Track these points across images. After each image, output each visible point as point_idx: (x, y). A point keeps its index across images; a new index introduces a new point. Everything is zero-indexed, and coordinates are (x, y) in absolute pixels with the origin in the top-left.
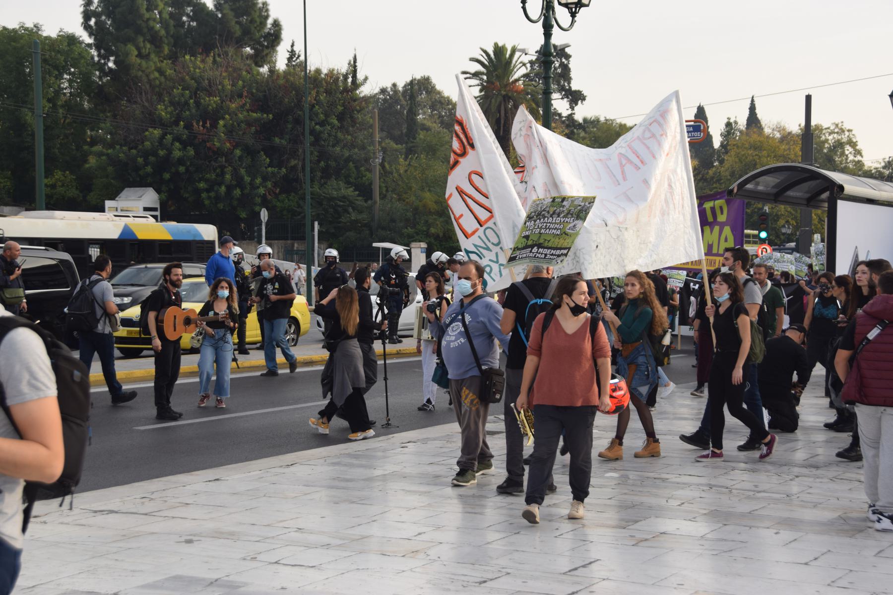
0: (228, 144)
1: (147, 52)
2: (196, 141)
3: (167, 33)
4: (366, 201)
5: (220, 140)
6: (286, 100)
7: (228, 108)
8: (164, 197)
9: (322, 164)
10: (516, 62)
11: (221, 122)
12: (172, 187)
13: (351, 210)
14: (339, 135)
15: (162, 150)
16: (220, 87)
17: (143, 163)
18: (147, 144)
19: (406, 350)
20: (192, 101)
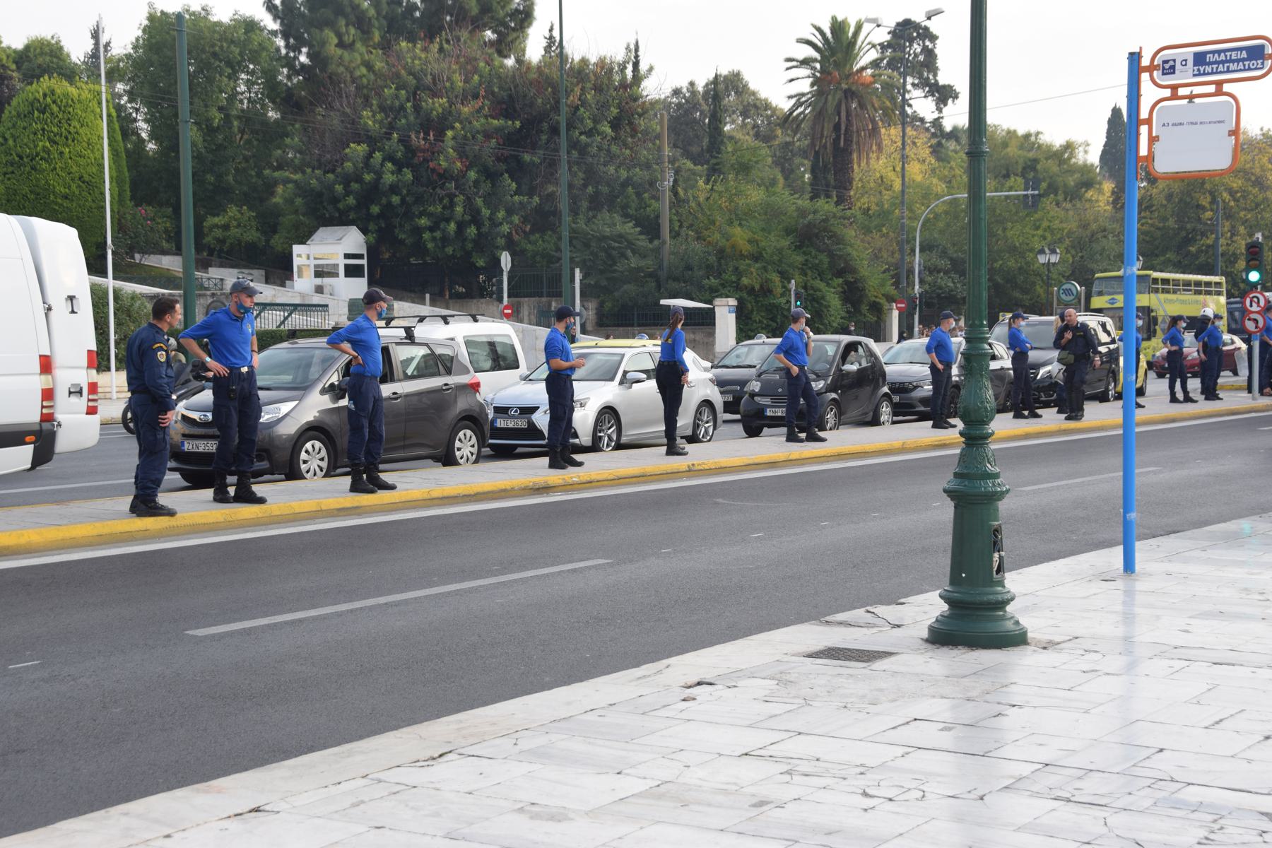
0: (459, 164)
2: (416, 161)
3: (378, 13)
4: (651, 241)
5: (448, 158)
6: (540, 101)
8: (371, 239)
9: (590, 189)
10: (863, 43)
11: (450, 133)
12: (383, 225)
13: (629, 253)
14: (614, 148)
15: (368, 173)
16: (448, 84)
18: (348, 165)
19: (704, 463)
20: (409, 105)
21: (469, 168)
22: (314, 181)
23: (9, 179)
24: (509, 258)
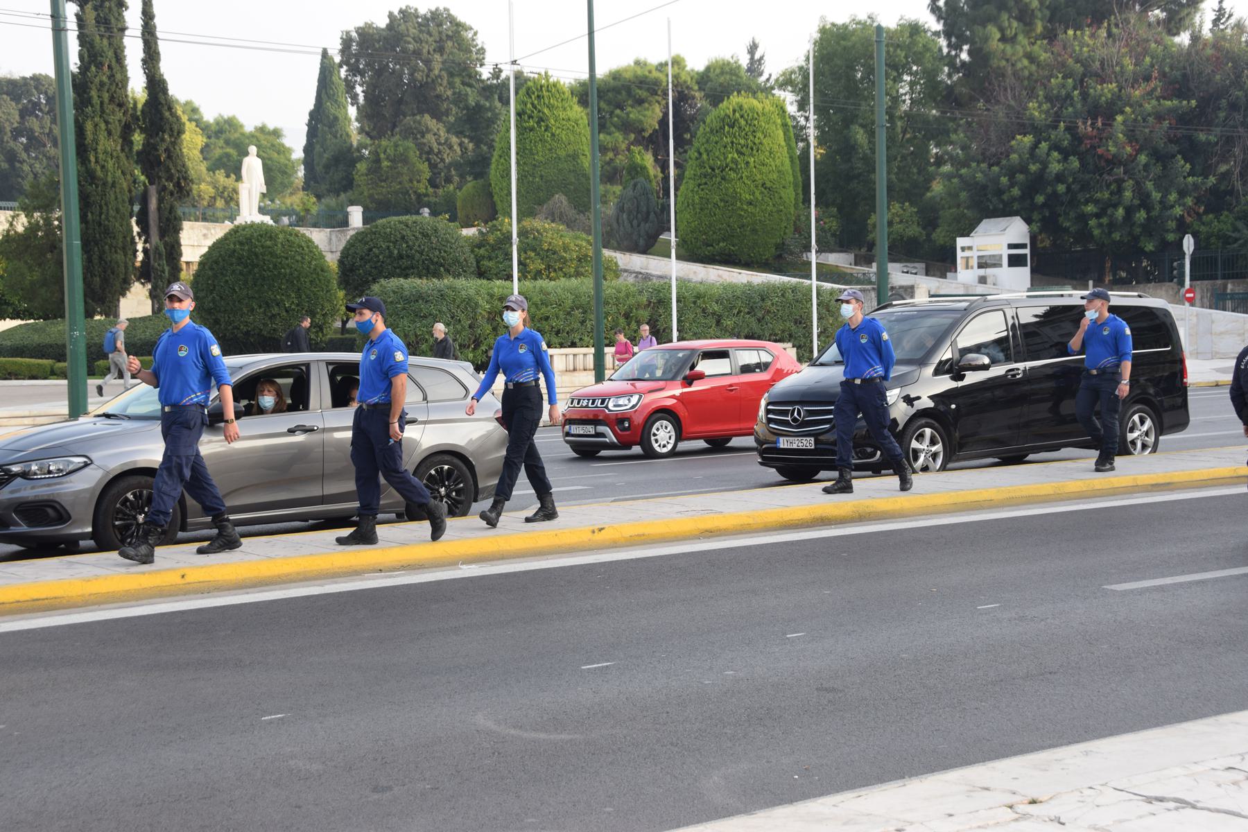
0: (1129, 149)
2: (1083, 148)
5: (1118, 143)
6: (1218, 77)
7: (1129, 97)
11: (1119, 118)
12: (1047, 214)
15: (1034, 164)
16: (1118, 69)
17: (1008, 183)
18: (1014, 156)
20: (1076, 93)
21: (1139, 152)
22: (979, 175)
23: (702, 190)
24: (1192, 241)
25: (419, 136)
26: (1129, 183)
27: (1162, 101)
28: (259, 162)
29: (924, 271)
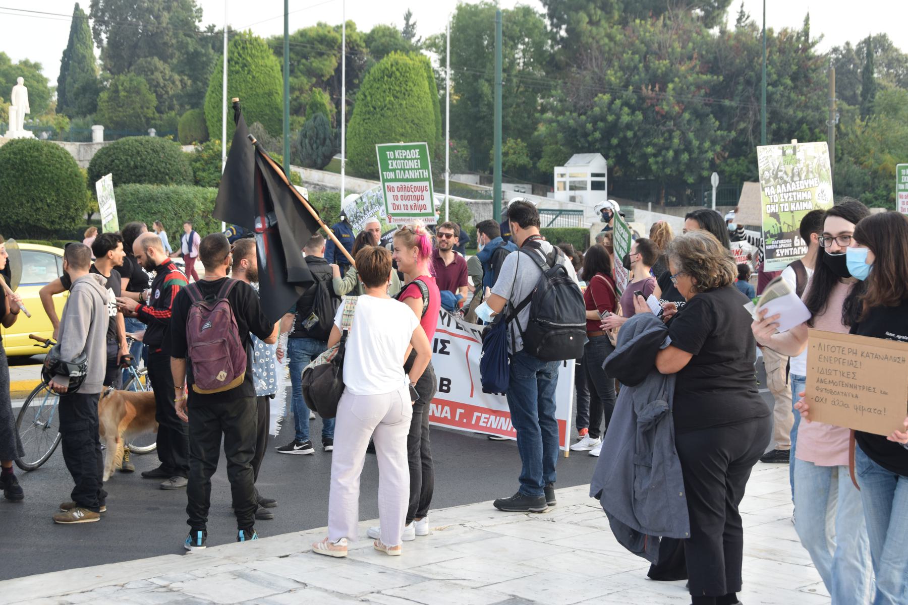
0: (677, 108)
1: (598, 18)
2: (645, 106)
5: (669, 104)
6: (738, 61)
7: (678, 71)
9: (774, 126)
11: (671, 86)
12: (620, 152)
14: (793, 95)
15: (611, 115)
16: (670, 50)
18: (597, 109)
21: (684, 110)
23: (366, 123)
25: (149, 73)
26: (677, 133)
27: (700, 75)
28: (25, 89)
29: (531, 191)
